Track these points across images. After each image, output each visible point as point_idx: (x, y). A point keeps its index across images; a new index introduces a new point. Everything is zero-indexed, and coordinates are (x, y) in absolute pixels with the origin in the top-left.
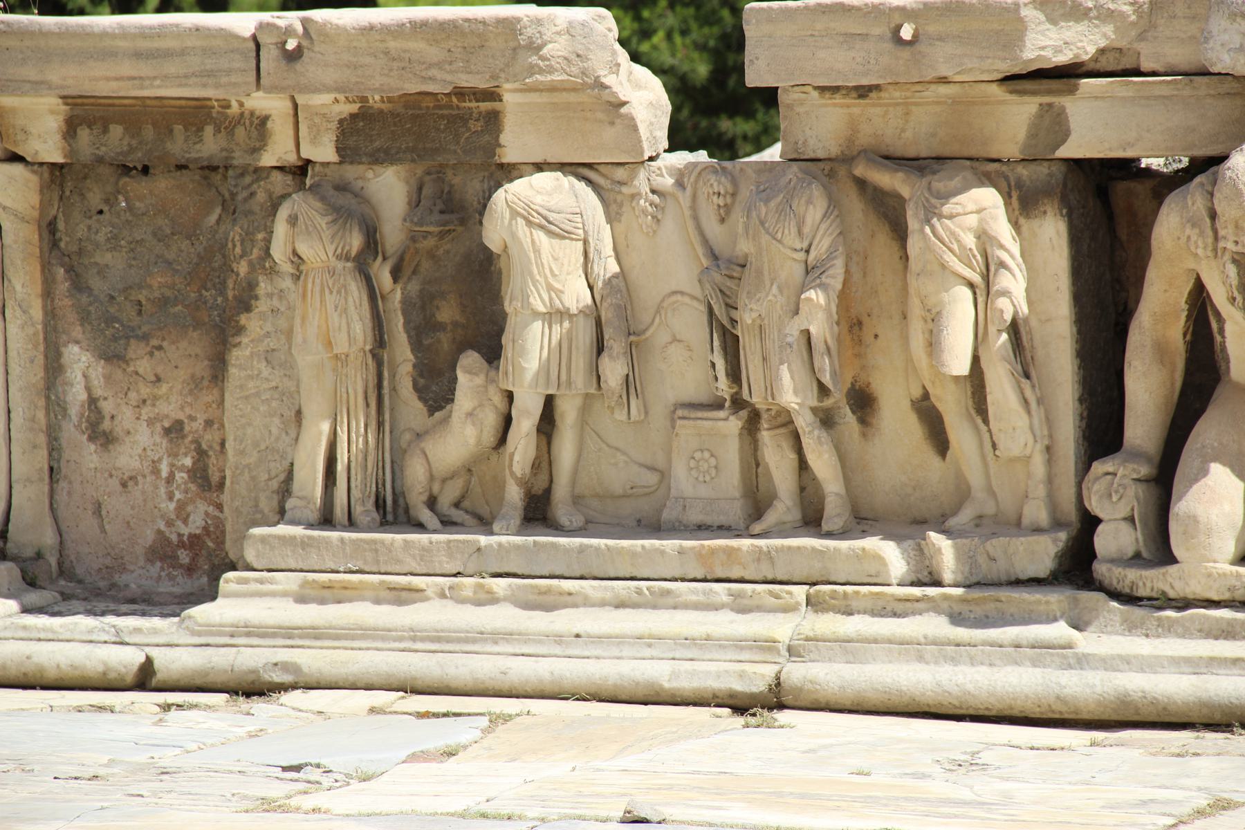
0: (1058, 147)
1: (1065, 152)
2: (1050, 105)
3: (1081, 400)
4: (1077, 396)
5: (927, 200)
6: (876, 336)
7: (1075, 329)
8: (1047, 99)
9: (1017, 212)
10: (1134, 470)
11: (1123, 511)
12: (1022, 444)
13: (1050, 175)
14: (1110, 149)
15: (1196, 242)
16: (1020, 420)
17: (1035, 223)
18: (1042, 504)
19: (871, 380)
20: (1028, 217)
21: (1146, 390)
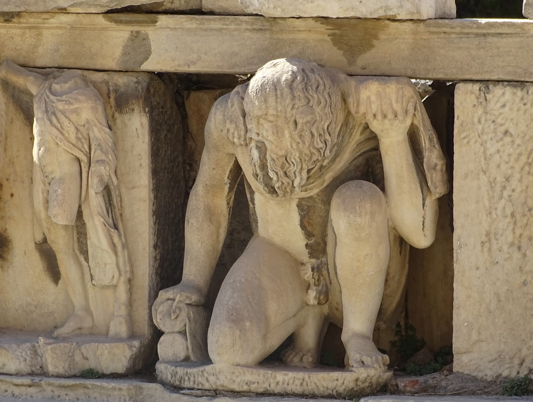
0: (142, 63)
1: (148, 66)
2: (138, 32)
3: (155, 246)
4: (152, 243)
5: (48, 97)
6: (12, 195)
7: (152, 196)
8: (136, 28)
9: (113, 109)
10: (187, 297)
11: (179, 326)
12: (111, 276)
13: (137, 82)
14: (179, 66)
15: (233, 134)
16: (109, 258)
17: (126, 117)
18: (124, 321)
19: (8, 227)
20: (121, 112)
21: (200, 240)
